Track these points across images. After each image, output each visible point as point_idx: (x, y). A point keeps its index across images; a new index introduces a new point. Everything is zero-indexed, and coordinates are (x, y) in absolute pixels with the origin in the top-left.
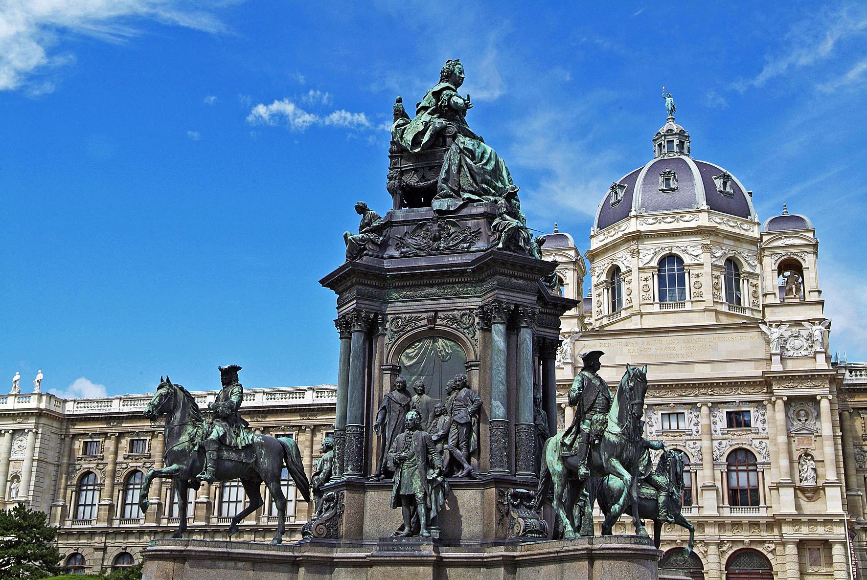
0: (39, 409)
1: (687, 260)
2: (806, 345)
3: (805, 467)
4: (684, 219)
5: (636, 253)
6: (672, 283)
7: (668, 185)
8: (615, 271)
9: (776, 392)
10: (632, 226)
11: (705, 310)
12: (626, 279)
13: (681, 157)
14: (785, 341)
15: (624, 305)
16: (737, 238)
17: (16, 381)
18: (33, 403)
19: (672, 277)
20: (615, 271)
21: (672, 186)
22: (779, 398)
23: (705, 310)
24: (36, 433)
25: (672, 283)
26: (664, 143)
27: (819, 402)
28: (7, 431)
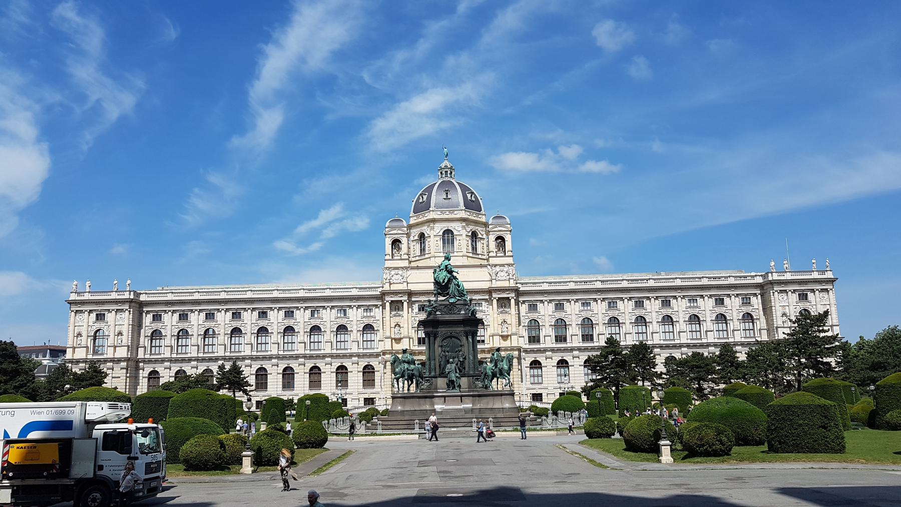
0: (130, 299)
1: (455, 233)
2: (506, 275)
3: (504, 327)
4: (455, 213)
5: (433, 228)
6: (448, 243)
7: (447, 196)
8: (422, 236)
9: (494, 296)
10: (431, 215)
11: (463, 256)
12: (428, 240)
13: (451, 180)
14: (497, 273)
15: (427, 252)
16: (476, 223)
17: (115, 284)
18: (126, 296)
19: (448, 240)
20: (422, 236)
21: (449, 197)
22: (495, 298)
23: (463, 256)
24: (130, 311)
25: (448, 243)
26: (444, 172)
27: (510, 300)
28: (113, 310)
